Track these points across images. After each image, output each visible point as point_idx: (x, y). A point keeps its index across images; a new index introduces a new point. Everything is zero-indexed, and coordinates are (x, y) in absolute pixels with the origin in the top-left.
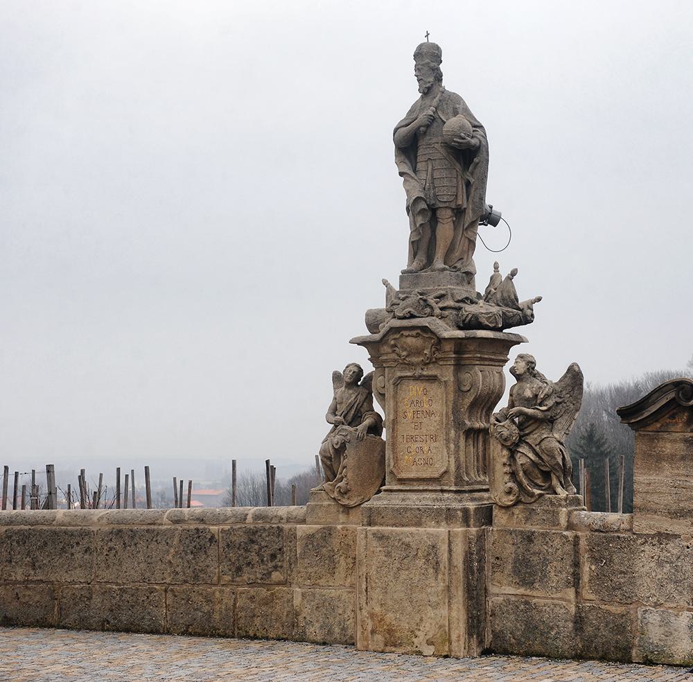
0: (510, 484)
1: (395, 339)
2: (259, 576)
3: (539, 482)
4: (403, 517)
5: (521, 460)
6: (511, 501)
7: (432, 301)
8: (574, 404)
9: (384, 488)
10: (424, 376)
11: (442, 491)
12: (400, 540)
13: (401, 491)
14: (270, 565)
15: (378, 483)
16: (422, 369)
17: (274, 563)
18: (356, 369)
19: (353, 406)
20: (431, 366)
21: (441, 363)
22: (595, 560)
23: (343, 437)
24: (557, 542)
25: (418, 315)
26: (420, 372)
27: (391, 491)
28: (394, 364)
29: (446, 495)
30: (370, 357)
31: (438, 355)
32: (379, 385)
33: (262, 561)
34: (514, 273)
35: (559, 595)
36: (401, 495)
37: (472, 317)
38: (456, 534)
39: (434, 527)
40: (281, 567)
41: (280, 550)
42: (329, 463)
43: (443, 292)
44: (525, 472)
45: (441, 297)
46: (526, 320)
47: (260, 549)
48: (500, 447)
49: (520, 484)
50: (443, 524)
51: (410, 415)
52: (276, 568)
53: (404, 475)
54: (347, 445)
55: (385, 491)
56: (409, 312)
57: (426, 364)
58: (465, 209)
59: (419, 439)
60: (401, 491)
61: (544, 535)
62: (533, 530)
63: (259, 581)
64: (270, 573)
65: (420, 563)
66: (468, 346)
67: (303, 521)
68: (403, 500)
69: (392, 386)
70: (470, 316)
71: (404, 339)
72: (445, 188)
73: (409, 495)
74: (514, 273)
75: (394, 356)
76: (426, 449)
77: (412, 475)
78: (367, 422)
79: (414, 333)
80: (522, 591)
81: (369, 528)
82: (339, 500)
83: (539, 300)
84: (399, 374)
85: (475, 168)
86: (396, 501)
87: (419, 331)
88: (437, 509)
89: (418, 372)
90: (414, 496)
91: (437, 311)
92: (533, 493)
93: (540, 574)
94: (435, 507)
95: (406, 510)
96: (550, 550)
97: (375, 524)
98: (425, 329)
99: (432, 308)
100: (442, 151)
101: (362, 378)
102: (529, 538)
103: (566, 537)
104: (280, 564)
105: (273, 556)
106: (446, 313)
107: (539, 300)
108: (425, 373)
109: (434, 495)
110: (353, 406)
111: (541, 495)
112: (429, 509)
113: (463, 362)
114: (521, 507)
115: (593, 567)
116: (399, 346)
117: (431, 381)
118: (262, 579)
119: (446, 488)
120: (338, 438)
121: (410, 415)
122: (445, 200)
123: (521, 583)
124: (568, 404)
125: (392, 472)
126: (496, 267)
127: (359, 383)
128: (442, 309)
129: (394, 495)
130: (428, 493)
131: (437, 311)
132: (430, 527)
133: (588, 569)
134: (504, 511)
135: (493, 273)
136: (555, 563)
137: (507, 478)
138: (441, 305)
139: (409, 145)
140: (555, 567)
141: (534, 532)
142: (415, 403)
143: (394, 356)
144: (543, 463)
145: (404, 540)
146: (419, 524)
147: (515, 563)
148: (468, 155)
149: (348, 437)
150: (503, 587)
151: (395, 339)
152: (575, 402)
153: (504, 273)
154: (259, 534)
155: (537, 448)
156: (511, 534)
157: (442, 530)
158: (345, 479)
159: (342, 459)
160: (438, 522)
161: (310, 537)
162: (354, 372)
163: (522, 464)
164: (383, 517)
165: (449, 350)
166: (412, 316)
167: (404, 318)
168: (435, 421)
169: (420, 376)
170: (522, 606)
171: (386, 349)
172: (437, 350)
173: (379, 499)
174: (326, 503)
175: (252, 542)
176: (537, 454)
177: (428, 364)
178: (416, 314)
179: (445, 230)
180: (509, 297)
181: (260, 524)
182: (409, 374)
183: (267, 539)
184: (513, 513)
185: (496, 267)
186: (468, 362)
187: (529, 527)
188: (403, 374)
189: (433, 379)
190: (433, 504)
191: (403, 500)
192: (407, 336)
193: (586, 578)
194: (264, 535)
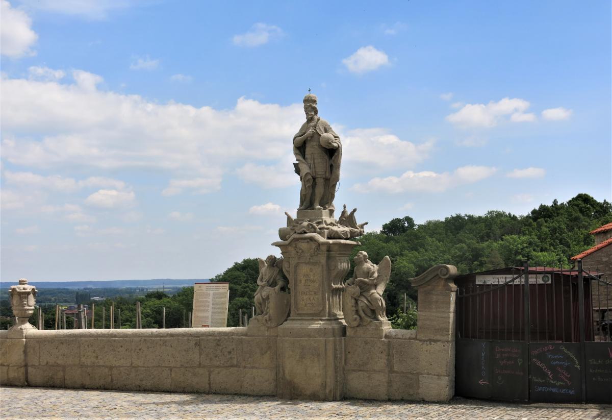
0: (356, 316)
5: (360, 304)
9: (290, 318)
17: (230, 356)
34: (355, 210)
44: (363, 311)
48: (350, 298)
51: (303, 282)
54: (270, 296)
60: (299, 320)
73: (304, 322)
74: (355, 210)
76: (312, 298)
79: (306, 241)
83: (366, 223)
85: (335, 158)
87: (309, 240)
98: (312, 239)
99: (315, 228)
104: (233, 356)
107: (366, 223)
121: (303, 282)
126: (345, 207)
128: (320, 229)
129: (294, 322)
135: (343, 210)
138: (320, 226)
139: (301, 147)
148: (332, 152)
153: (349, 212)
158: (268, 314)
159: (267, 303)
171: (290, 248)
173: (288, 324)
176: (369, 301)
179: (319, 190)
185: (345, 207)
189: (315, 264)
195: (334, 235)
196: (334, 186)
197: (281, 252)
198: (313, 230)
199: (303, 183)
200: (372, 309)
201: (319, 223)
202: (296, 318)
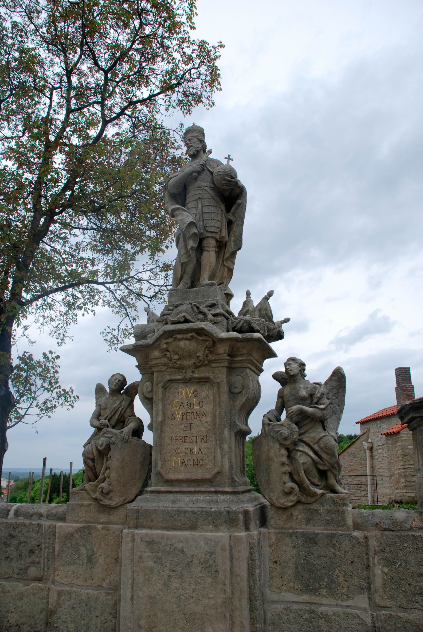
0: (291, 484)
1: (167, 343)
2: (16, 571)
3: (316, 481)
4: (175, 520)
5: (302, 459)
6: (292, 502)
7: (203, 308)
8: (339, 405)
10: (195, 378)
11: (216, 492)
12: (171, 545)
13: (170, 492)
14: (29, 560)
15: (140, 484)
16: (193, 372)
17: (31, 559)
18: (121, 378)
19: (117, 411)
20: (202, 368)
21: (214, 365)
22: (389, 563)
23: (107, 439)
24: (346, 544)
25: (191, 320)
26: (191, 374)
27: (159, 492)
28: (164, 368)
29: (221, 497)
30: (137, 364)
31: (210, 357)
32: (145, 390)
33: (20, 556)
35: (350, 603)
36: (171, 497)
37: (244, 323)
38: (239, 540)
39: (211, 531)
40: (39, 563)
41: (38, 546)
42: (91, 464)
43: (215, 302)
44: (305, 471)
45: (213, 306)
46: (280, 336)
47: (19, 544)
48: (277, 446)
49: (300, 485)
50: (222, 528)
51: (179, 417)
52: (33, 563)
53: (172, 476)
54: (112, 447)
55: (152, 492)
56: (184, 317)
57: (197, 367)
58: (226, 242)
59: (188, 440)
61: (331, 537)
62: (316, 531)
63: (15, 576)
64: (27, 569)
65: (196, 569)
66: (240, 349)
67: (63, 519)
68: (174, 502)
69: (161, 390)
70: (242, 322)
71: (176, 343)
72: (212, 221)
73: (180, 497)
75: (165, 360)
76: (196, 450)
77: (181, 476)
78: (131, 425)
79: (189, 335)
80: (305, 597)
81: (136, 531)
82: (101, 500)
84: (168, 378)
85: (237, 209)
86: (165, 503)
87: (194, 334)
88: (215, 512)
89: (189, 374)
90: (187, 498)
91: (210, 317)
92: (315, 493)
93: (326, 579)
94: (213, 510)
95: (179, 512)
96: (337, 553)
97: (143, 527)
98: (200, 332)
100: (211, 192)
101: (125, 388)
102: (311, 539)
103: (356, 538)
104: (37, 560)
105: (32, 552)
106: (219, 319)
108: (196, 375)
109: (208, 497)
110: (117, 411)
111: (323, 494)
112: (205, 511)
113: (234, 366)
114: (300, 507)
115: (386, 570)
116: (170, 350)
117: (202, 383)
118: (18, 574)
119: (220, 489)
120: (102, 440)
121: (179, 417)
122: (212, 231)
123: (304, 589)
124: (335, 405)
125: (159, 474)
126: (248, 294)
127: (122, 392)
128: (214, 315)
129: (162, 497)
130: (200, 495)
131: (210, 317)
132: (206, 531)
133: (380, 572)
134: (281, 512)
135: (245, 299)
136: (344, 567)
137: (286, 478)
138: (214, 312)
140: (345, 572)
141: (318, 534)
142: (185, 405)
143: (165, 360)
144: (322, 462)
145: (176, 545)
146: (193, 528)
147: (297, 568)
149: (113, 439)
150: (282, 594)
151: (167, 343)
152: (340, 404)
154: (19, 529)
155: (316, 447)
156: (291, 536)
157: (222, 535)
158: (107, 480)
160: (216, 526)
161: (69, 536)
162: (119, 380)
163: (303, 463)
164: (152, 520)
165: (223, 352)
166: (186, 321)
167: (179, 322)
168: (207, 422)
169: (191, 379)
170: (307, 615)
172: (211, 352)
173: (147, 500)
174: (86, 503)
175: (12, 536)
177: (200, 366)
178: (190, 318)
179: (210, 257)
180: (267, 314)
181: (21, 520)
182: (179, 377)
183: (27, 535)
184: (292, 514)
186: (239, 365)
187: (311, 529)
188: (173, 377)
189: (204, 381)
190: (210, 506)
191: (174, 502)
192: (179, 340)
193: (378, 582)
194: (24, 531)
195: (241, 327)
196: (233, 254)
197: (137, 364)
198: (201, 316)
199: (183, 251)
200: (321, 467)
201: (213, 306)
202: (163, 489)
